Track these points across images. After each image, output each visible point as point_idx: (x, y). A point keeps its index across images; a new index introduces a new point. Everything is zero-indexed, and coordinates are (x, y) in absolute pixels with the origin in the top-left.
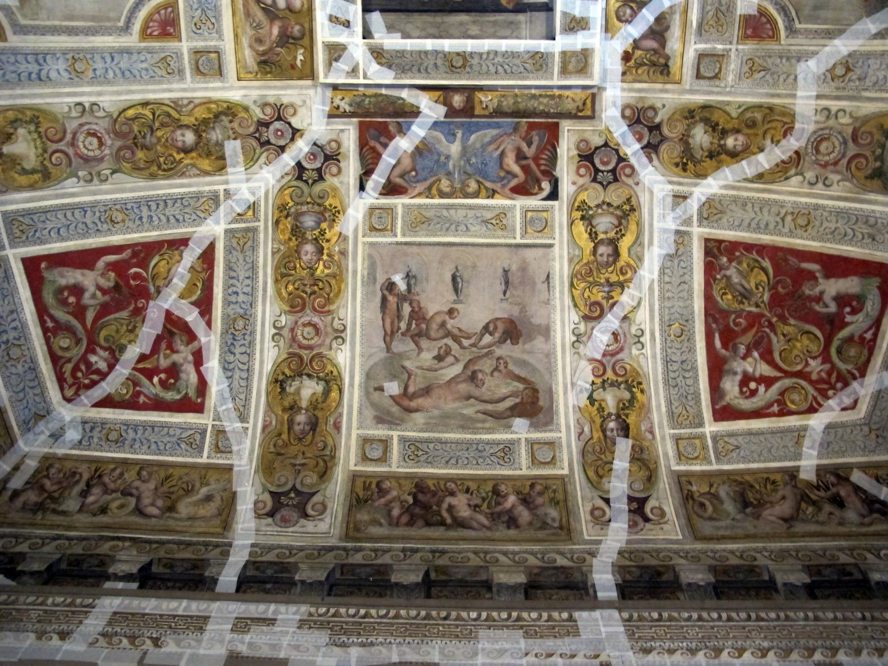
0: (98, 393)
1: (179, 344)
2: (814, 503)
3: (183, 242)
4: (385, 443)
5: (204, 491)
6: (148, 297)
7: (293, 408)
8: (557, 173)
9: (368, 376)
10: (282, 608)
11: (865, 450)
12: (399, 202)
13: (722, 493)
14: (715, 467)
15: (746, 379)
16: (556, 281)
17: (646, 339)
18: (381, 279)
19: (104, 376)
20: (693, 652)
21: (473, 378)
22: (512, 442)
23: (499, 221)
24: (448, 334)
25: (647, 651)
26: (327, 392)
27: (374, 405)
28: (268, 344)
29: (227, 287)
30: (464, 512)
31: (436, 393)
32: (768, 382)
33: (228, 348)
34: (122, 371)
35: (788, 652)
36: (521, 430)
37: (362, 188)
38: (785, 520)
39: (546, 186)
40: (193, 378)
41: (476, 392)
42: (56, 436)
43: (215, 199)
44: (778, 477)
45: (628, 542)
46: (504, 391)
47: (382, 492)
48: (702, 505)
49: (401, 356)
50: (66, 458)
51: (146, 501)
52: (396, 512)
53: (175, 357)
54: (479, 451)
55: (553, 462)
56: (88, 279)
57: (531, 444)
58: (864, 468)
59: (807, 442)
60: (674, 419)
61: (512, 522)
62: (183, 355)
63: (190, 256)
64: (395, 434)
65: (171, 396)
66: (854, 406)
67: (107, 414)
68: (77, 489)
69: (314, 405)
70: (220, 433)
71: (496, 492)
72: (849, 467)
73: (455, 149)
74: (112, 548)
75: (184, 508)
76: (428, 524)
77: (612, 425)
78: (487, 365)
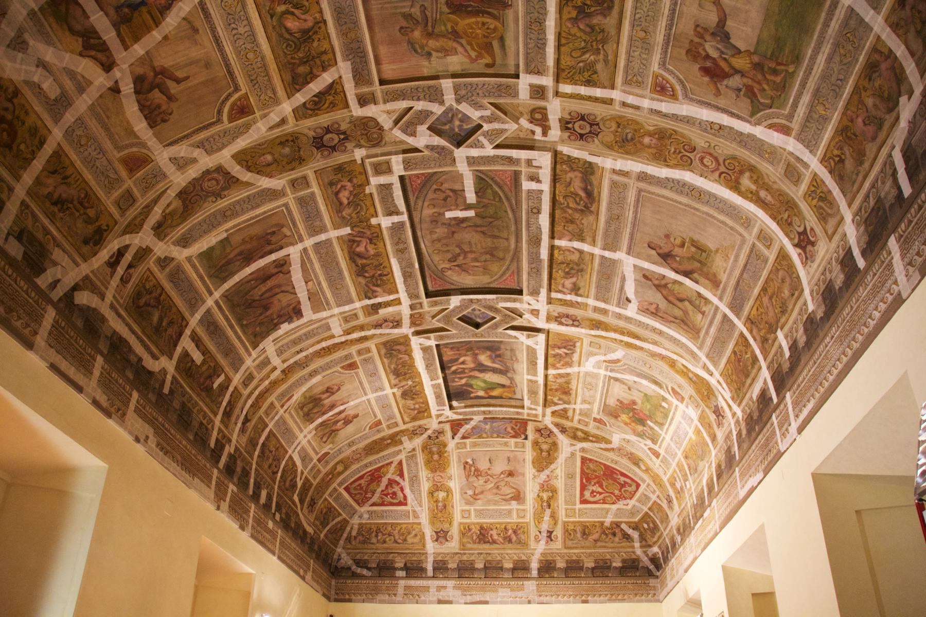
0: (371, 502)
1: (394, 485)
2: (606, 534)
3: (392, 462)
4: (469, 511)
5: (414, 533)
6: (381, 477)
7: (437, 501)
8: (527, 433)
9: (461, 489)
10: (448, 582)
11: (628, 517)
12: (468, 441)
13: (578, 530)
14: (577, 520)
15: (593, 492)
16: (527, 461)
17: (559, 477)
18: (463, 461)
19: (371, 498)
20: (552, 596)
21: (498, 487)
22: (511, 510)
23: (506, 444)
24: (488, 475)
25: (540, 596)
26: (448, 496)
27: (464, 498)
28: (425, 482)
29: (408, 470)
30: (495, 537)
31: (485, 493)
32: (600, 493)
33: (412, 484)
34: (377, 495)
35: (576, 595)
36: (514, 505)
37: (453, 438)
38: (595, 541)
39: (523, 437)
40: (402, 495)
41: (499, 492)
42: (361, 517)
43: (400, 451)
44: (597, 524)
45: (545, 549)
46: (509, 492)
47: (470, 530)
48: (570, 534)
49: (472, 482)
50: (366, 524)
51: (397, 537)
52: (475, 538)
53: (394, 490)
54: (500, 513)
55: (524, 517)
56: (362, 482)
57: (518, 510)
58: (626, 523)
59: (610, 513)
60: (566, 503)
61: (510, 541)
62: (396, 489)
63: (393, 466)
64: (472, 508)
65: (395, 501)
66: (627, 505)
67: (375, 508)
68: (374, 535)
69: (444, 500)
70: (414, 511)
71: (505, 528)
72: (621, 522)
73: (488, 427)
74: (393, 557)
75: (410, 539)
76: (485, 543)
77: (545, 504)
78: (503, 484)
